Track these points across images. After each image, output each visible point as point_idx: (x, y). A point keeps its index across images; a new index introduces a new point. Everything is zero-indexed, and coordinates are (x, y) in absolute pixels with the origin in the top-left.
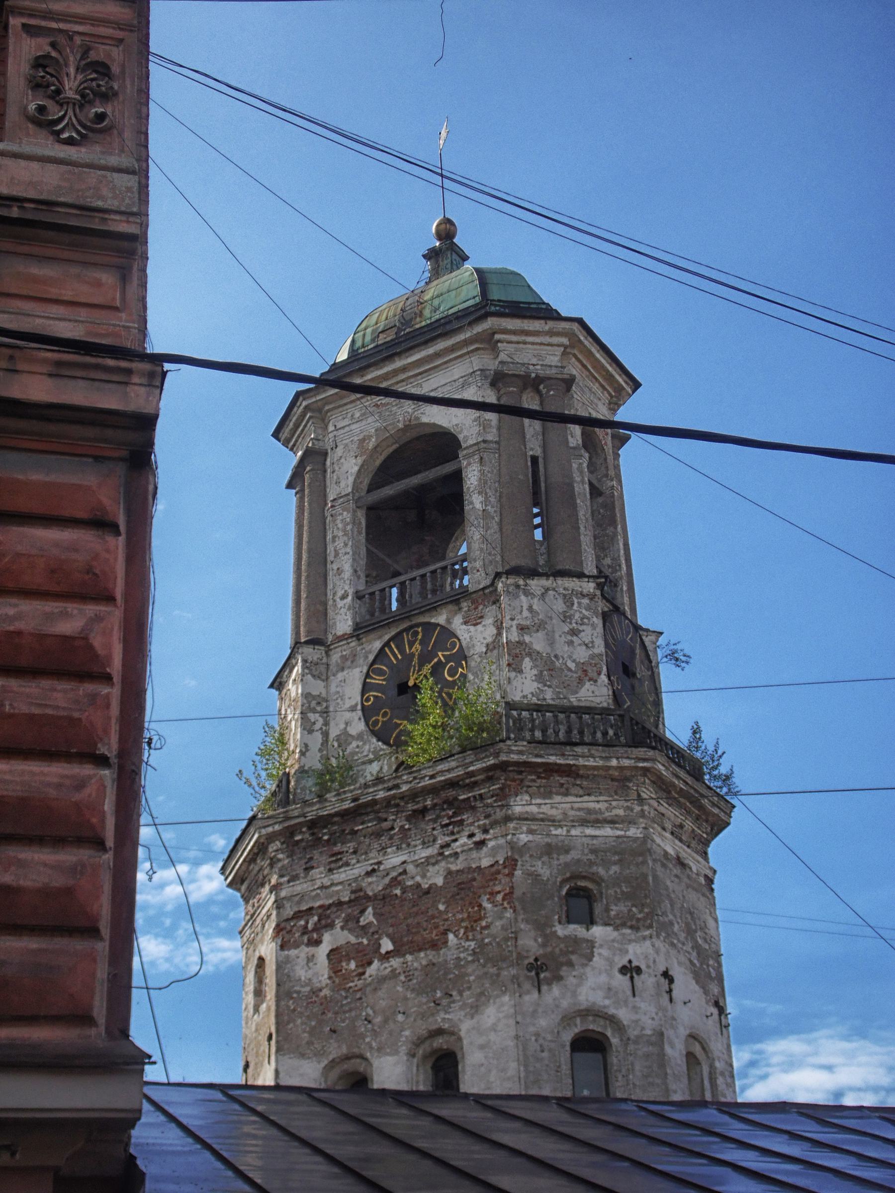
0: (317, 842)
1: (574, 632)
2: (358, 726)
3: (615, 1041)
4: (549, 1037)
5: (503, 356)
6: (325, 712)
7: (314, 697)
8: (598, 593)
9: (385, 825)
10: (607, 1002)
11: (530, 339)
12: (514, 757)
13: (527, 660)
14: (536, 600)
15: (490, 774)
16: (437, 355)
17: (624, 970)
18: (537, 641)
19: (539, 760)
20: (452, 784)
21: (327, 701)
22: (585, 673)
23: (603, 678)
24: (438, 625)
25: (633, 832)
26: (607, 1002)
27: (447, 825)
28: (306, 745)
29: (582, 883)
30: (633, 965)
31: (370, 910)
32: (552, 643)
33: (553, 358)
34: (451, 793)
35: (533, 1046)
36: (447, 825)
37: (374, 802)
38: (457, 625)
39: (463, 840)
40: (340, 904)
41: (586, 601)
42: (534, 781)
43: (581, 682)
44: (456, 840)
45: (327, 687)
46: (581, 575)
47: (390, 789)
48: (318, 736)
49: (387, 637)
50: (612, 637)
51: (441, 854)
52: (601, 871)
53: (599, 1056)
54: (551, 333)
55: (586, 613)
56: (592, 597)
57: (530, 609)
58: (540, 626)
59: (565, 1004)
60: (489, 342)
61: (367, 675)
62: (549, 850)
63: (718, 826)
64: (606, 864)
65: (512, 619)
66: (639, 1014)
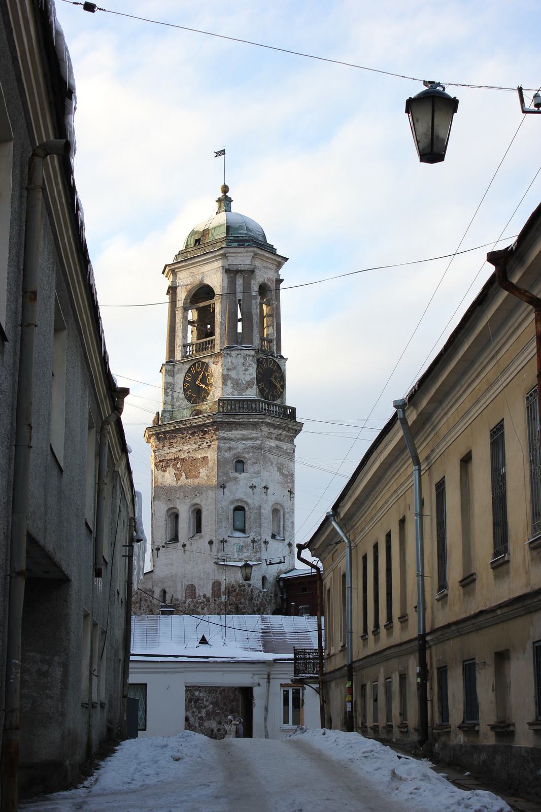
0: (165, 438)
1: (246, 370)
2: (182, 395)
3: (246, 508)
4: (225, 508)
5: (230, 262)
7: (169, 383)
8: (256, 354)
9: (185, 435)
10: (244, 497)
11: (239, 255)
12: (219, 420)
13: (229, 381)
14: (234, 359)
15: (212, 424)
16: (209, 258)
17: (251, 487)
18: (233, 374)
19: (227, 420)
20: (202, 425)
21: (172, 384)
22: (249, 385)
23: (255, 387)
24: (205, 363)
25: (258, 442)
26: (244, 497)
27: (201, 438)
28: (166, 401)
29: (240, 459)
30: (254, 485)
31: (180, 463)
32: (238, 374)
33: (248, 261)
34: (202, 428)
35: (221, 511)
36: (200, 438)
37: (180, 428)
39: (205, 444)
40: (172, 459)
41: (251, 358)
42: (226, 426)
43: (247, 388)
44: (203, 444)
45: (174, 379)
47: (184, 425)
48: (170, 397)
49: (191, 364)
50: (262, 369)
51: (199, 448)
52: (246, 456)
53: (243, 512)
54: (247, 252)
55: (251, 362)
56: (253, 356)
57: (232, 362)
58: (234, 368)
59: (231, 498)
60: (224, 256)
61: (185, 377)
62: (230, 449)
63: (297, 432)
64: (248, 453)
65: (225, 366)
66: (253, 501)
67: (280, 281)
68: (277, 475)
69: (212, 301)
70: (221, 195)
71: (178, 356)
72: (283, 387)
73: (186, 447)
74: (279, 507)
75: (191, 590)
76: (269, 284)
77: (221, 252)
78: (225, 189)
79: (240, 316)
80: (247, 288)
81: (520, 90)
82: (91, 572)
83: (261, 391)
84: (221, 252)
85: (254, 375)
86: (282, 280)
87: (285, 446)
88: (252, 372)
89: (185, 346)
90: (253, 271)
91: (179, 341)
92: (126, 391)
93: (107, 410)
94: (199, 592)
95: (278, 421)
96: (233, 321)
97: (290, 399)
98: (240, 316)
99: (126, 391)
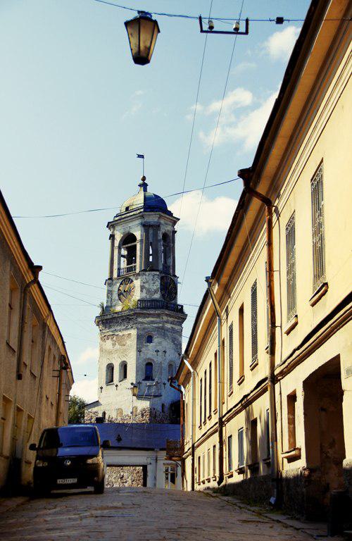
1: (154, 283)
6: (112, 294)
18: (146, 285)
22: (156, 292)
38: (134, 279)
46: (158, 270)
48: (110, 299)
58: (147, 282)
60: (142, 217)
62: (144, 329)
66: (157, 359)
67: (174, 232)
68: (172, 345)
69: (133, 244)
70: (142, 182)
71: (115, 275)
72: (176, 293)
73: (119, 328)
74: (172, 363)
75: (120, 411)
76: (168, 233)
77: (141, 214)
78: (144, 179)
79: (151, 253)
80: (155, 235)
81: (200, 18)
82: (14, 375)
83: (163, 295)
84: (141, 214)
85: (159, 286)
86: (176, 232)
87: (177, 327)
88: (158, 284)
89: (119, 269)
90: (159, 226)
91: (116, 266)
92: (40, 268)
93: (29, 278)
94: (124, 413)
95: (172, 313)
96: (147, 255)
97: (181, 300)
98: (151, 253)
99: (40, 268)
